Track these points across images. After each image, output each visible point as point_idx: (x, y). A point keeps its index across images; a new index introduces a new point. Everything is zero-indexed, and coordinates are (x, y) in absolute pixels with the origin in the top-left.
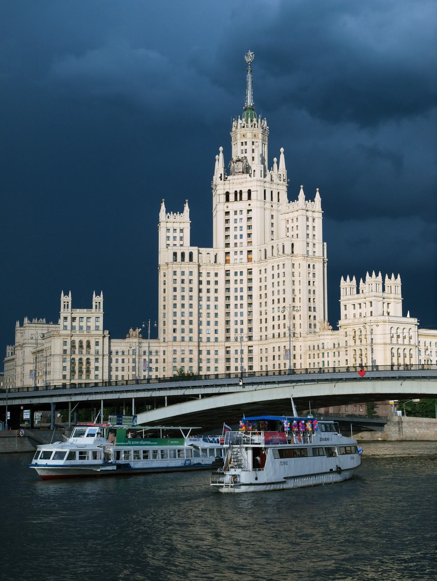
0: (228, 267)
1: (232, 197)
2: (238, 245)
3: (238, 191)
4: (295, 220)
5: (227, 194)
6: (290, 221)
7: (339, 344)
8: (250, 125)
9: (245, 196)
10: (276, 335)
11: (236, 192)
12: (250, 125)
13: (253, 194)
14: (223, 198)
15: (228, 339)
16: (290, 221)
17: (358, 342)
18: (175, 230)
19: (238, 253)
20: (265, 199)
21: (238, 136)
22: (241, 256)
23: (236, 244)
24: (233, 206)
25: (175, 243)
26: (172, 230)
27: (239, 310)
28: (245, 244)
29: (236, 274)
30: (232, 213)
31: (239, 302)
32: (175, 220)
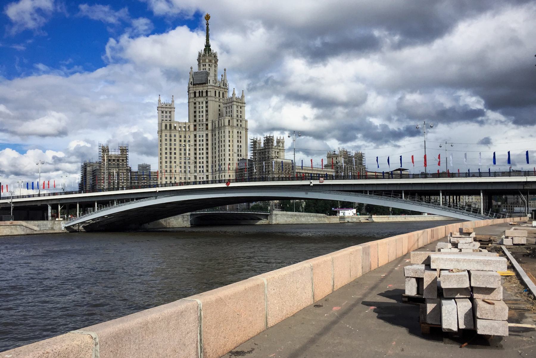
1: (197, 95)
2: (201, 121)
3: (201, 91)
5: (195, 93)
6: (228, 108)
8: (207, 55)
9: (204, 94)
11: (200, 91)
12: (207, 55)
13: (209, 94)
14: (192, 95)
15: (195, 171)
16: (228, 108)
18: (166, 112)
19: (201, 125)
20: (215, 95)
21: (201, 61)
22: (202, 127)
23: (200, 120)
25: (166, 119)
26: (164, 112)
27: (201, 156)
28: (204, 120)
29: (200, 137)
30: (197, 103)
31: (201, 152)
32: (166, 107)
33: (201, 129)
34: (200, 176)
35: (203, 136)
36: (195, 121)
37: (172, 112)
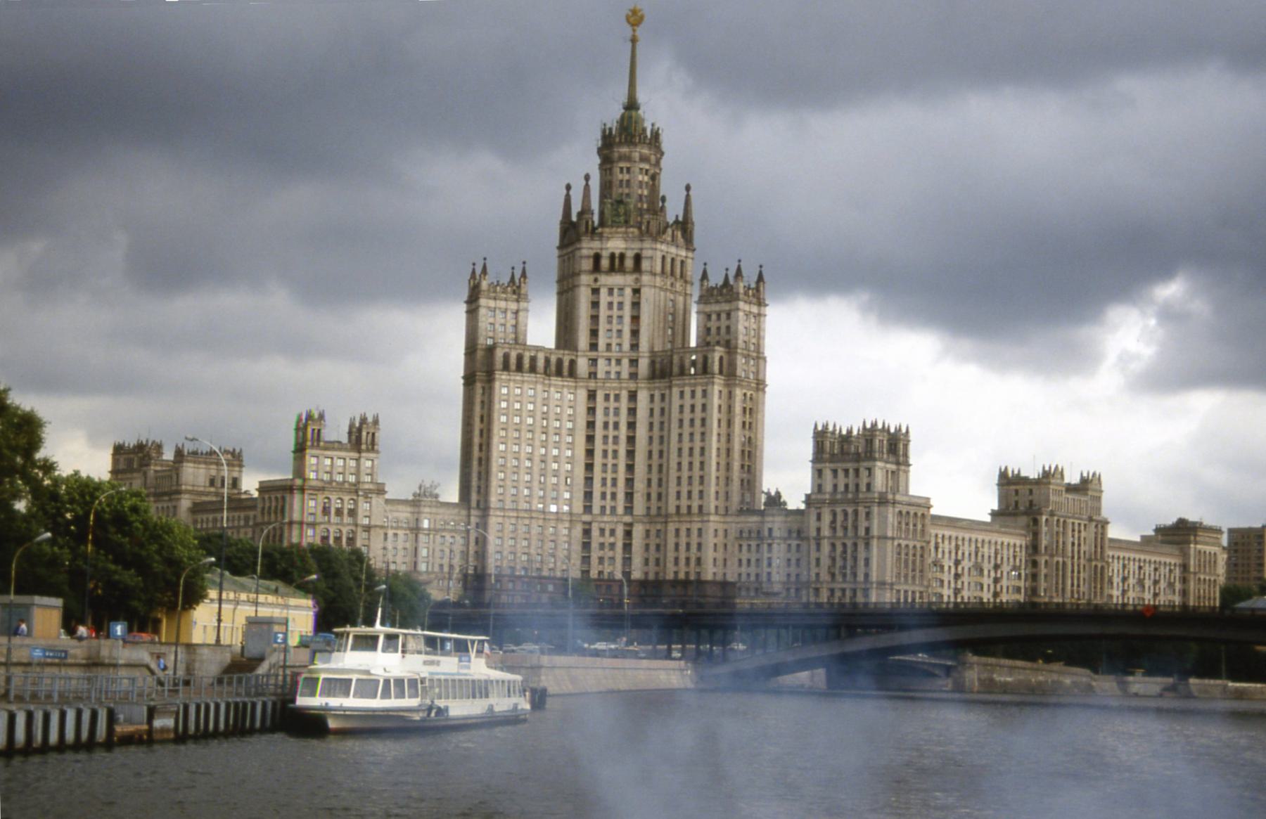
0: (592, 385)
1: (605, 263)
3: (617, 255)
4: (723, 316)
5: (597, 258)
6: (714, 317)
7: (799, 532)
9: (629, 263)
10: (684, 510)
13: (645, 265)
14: (587, 265)
16: (714, 317)
17: (840, 533)
24: (607, 280)
28: (626, 346)
29: (607, 397)
30: (604, 292)
33: (613, 376)
34: (602, 525)
35: (617, 397)
36: (594, 346)
37: (521, 314)
